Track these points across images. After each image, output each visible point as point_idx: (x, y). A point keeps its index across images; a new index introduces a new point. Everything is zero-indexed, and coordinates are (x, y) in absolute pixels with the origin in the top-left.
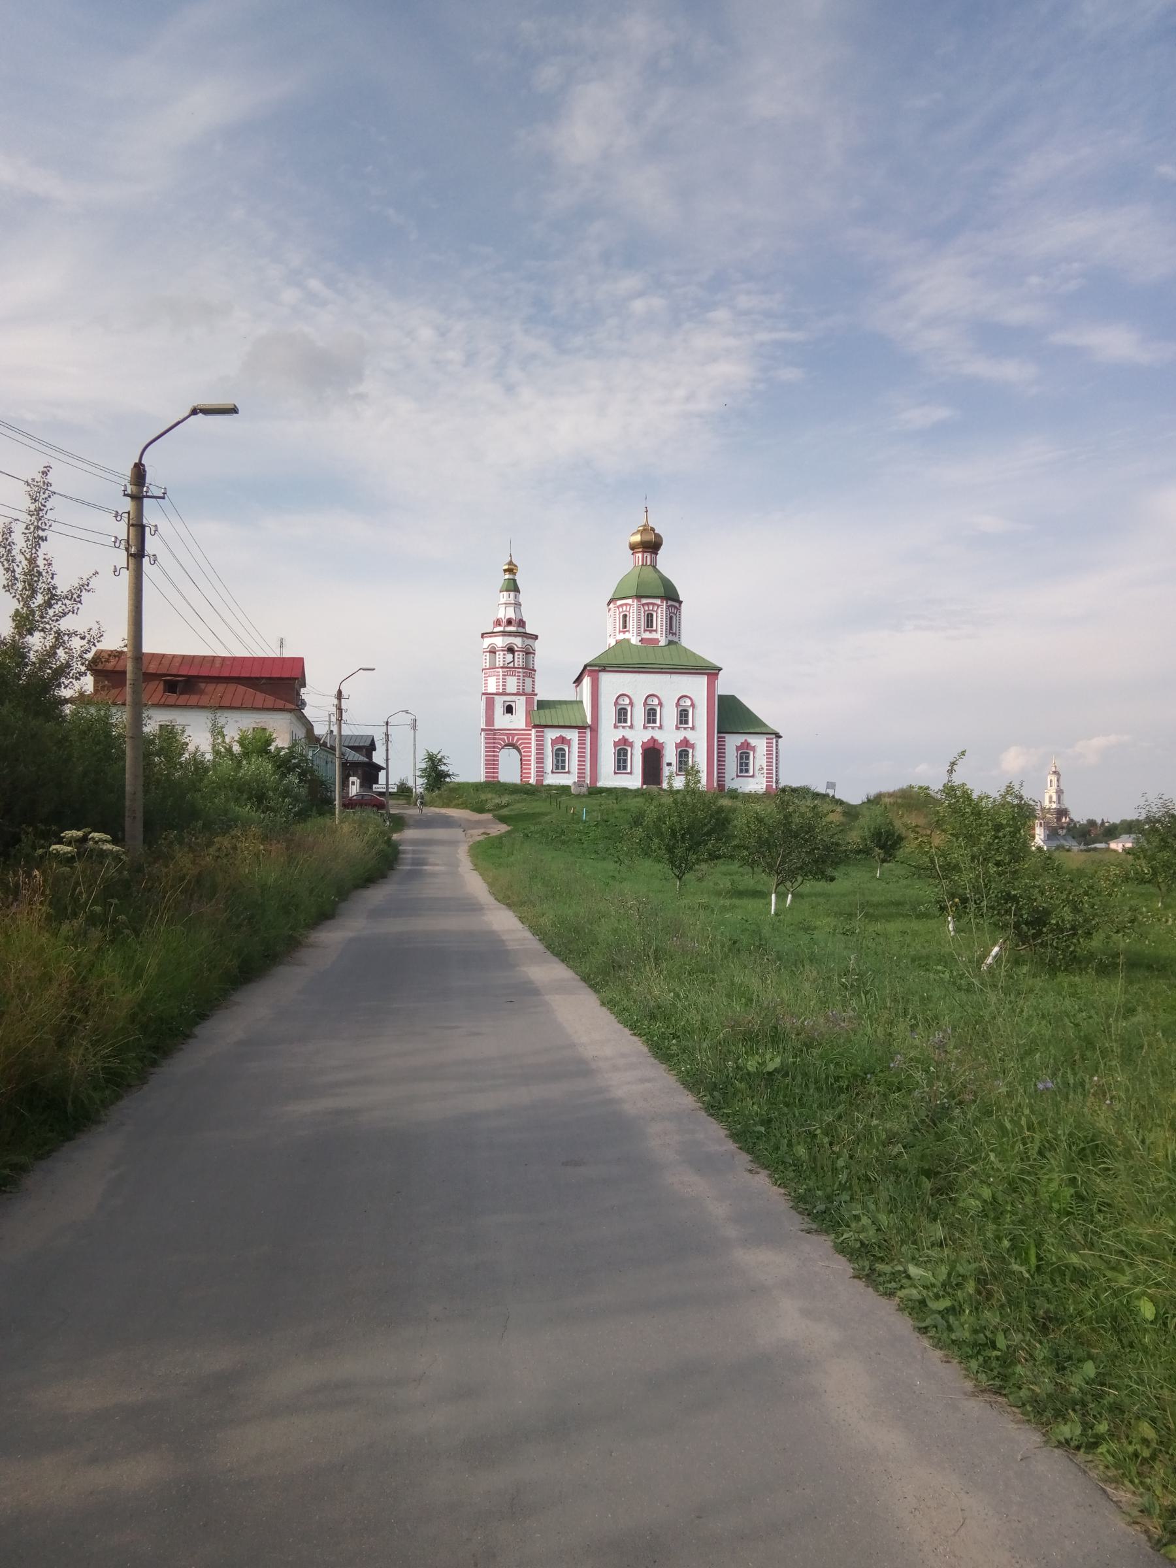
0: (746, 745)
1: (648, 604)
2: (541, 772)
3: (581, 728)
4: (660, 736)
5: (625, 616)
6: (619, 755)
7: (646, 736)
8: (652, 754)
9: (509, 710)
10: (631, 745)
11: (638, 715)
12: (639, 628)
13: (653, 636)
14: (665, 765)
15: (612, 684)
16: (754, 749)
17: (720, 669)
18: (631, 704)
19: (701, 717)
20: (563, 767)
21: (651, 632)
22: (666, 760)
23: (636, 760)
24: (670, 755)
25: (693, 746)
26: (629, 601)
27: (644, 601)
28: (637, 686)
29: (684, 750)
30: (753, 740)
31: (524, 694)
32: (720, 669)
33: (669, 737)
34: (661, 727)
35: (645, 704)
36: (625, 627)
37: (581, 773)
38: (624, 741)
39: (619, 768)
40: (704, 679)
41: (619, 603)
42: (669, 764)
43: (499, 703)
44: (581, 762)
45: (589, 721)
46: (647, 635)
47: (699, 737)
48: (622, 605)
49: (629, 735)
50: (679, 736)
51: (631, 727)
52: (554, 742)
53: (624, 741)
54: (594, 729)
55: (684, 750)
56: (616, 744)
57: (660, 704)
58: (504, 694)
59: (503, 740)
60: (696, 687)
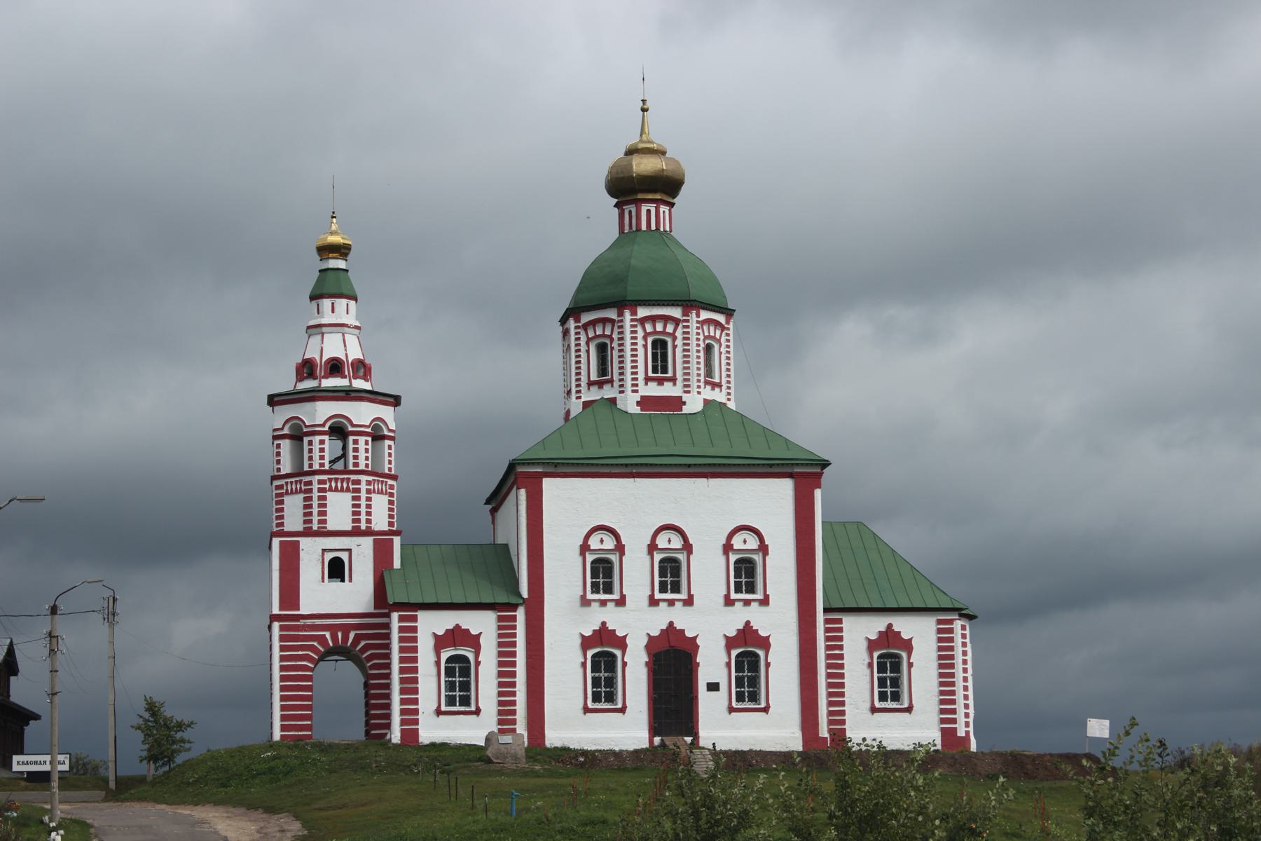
0: (889, 638)
1: (653, 319)
2: (411, 716)
4: (686, 621)
7: (656, 620)
8: (673, 661)
10: (622, 643)
11: (637, 574)
13: (668, 390)
15: (571, 507)
16: (908, 646)
17: (825, 464)
19: (780, 572)
21: (660, 382)
22: (703, 679)
24: (713, 664)
25: (765, 643)
28: (634, 508)
29: (748, 651)
30: (906, 626)
31: (368, 532)
32: (825, 464)
33: (709, 624)
36: (603, 370)
40: (784, 489)
41: (586, 318)
42: (713, 687)
43: (312, 553)
46: (653, 390)
48: (593, 323)
49: (617, 620)
50: (733, 621)
52: (441, 642)
55: (748, 651)
56: (586, 643)
59: (322, 640)
60: (768, 504)
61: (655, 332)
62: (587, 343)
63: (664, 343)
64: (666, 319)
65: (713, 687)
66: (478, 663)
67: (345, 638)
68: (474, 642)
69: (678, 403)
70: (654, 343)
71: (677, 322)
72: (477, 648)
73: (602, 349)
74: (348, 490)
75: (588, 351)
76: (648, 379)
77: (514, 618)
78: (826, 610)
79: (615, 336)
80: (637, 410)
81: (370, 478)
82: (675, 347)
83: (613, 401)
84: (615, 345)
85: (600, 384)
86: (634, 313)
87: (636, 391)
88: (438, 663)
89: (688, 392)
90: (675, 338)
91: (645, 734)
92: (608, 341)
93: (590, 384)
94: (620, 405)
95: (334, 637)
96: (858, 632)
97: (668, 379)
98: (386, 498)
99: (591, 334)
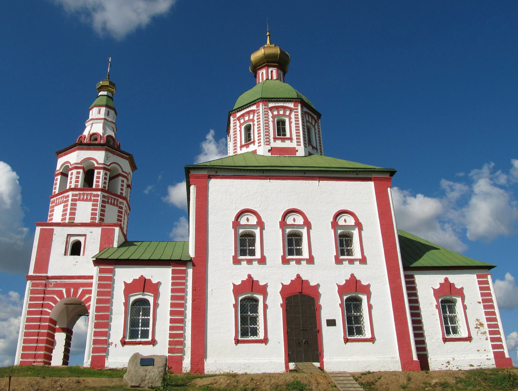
1: (277, 108)
3: (178, 263)
4: (310, 275)
5: (248, 129)
6: (243, 310)
7: (288, 274)
9: (76, 249)
11: (273, 242)
12: (267, 135)
13: (287, 144)
14: (324, 323)
18: (261, 224)
20: (145, 334)
21: (283, 140)
22: (325, 315)
23: (273, 317)
24: (330, 306)
26: (254, 108)
27: (271, 105)
29: (353, 297)
33: (327, 277)
34: (311, 260)
35: (283, 224)
37: (176, 341)
38: (251, 284)
39: (244, 333)
42: (331, 323)
44: (177, 322)
45: (192, 253)
46: (279, 144)
47: (375, 273)
48: (243, 116)
49: (259, 274)
51: (262, 261)
52: (129, 289)
53: (251, 284)
54: (200, 263)
55: (353, 297)
56: (237, 290)
57: (307, 224)
58: (72, 224)
61: (279, 115)
62: (240, 127)
63: (284, 123)
64: (285, 108)
65: (331, 323)
66: (156, 305)
67: (76, 293)
68: (154, 288)
69: (293, 151)
70: (278, 123)
71: (291, 110)
72: (156, 296)
73: (248, 129)
74: (90, 200)
75: (240, 131)
76: (275, 139)
77: (185, 272)
78: (405, 269)
79: (255, 118)
80: (269, 154)
81: (106, 194)
82: (290, 123)
83: (255, 152)
84: (256, 123)
85: (247, 146)
86: (266, 105)
87: (269, 145)
88: (126, 304)
89: (300, 145)
90: (290, 118)
91: (282, 359)
92: (251, 123)
93: (242, 146)
94: (259, 153)
95: (68, 292)
96: (427, 284)
97: (288, 139)
98: (117, 209)
99: (242, 121)
